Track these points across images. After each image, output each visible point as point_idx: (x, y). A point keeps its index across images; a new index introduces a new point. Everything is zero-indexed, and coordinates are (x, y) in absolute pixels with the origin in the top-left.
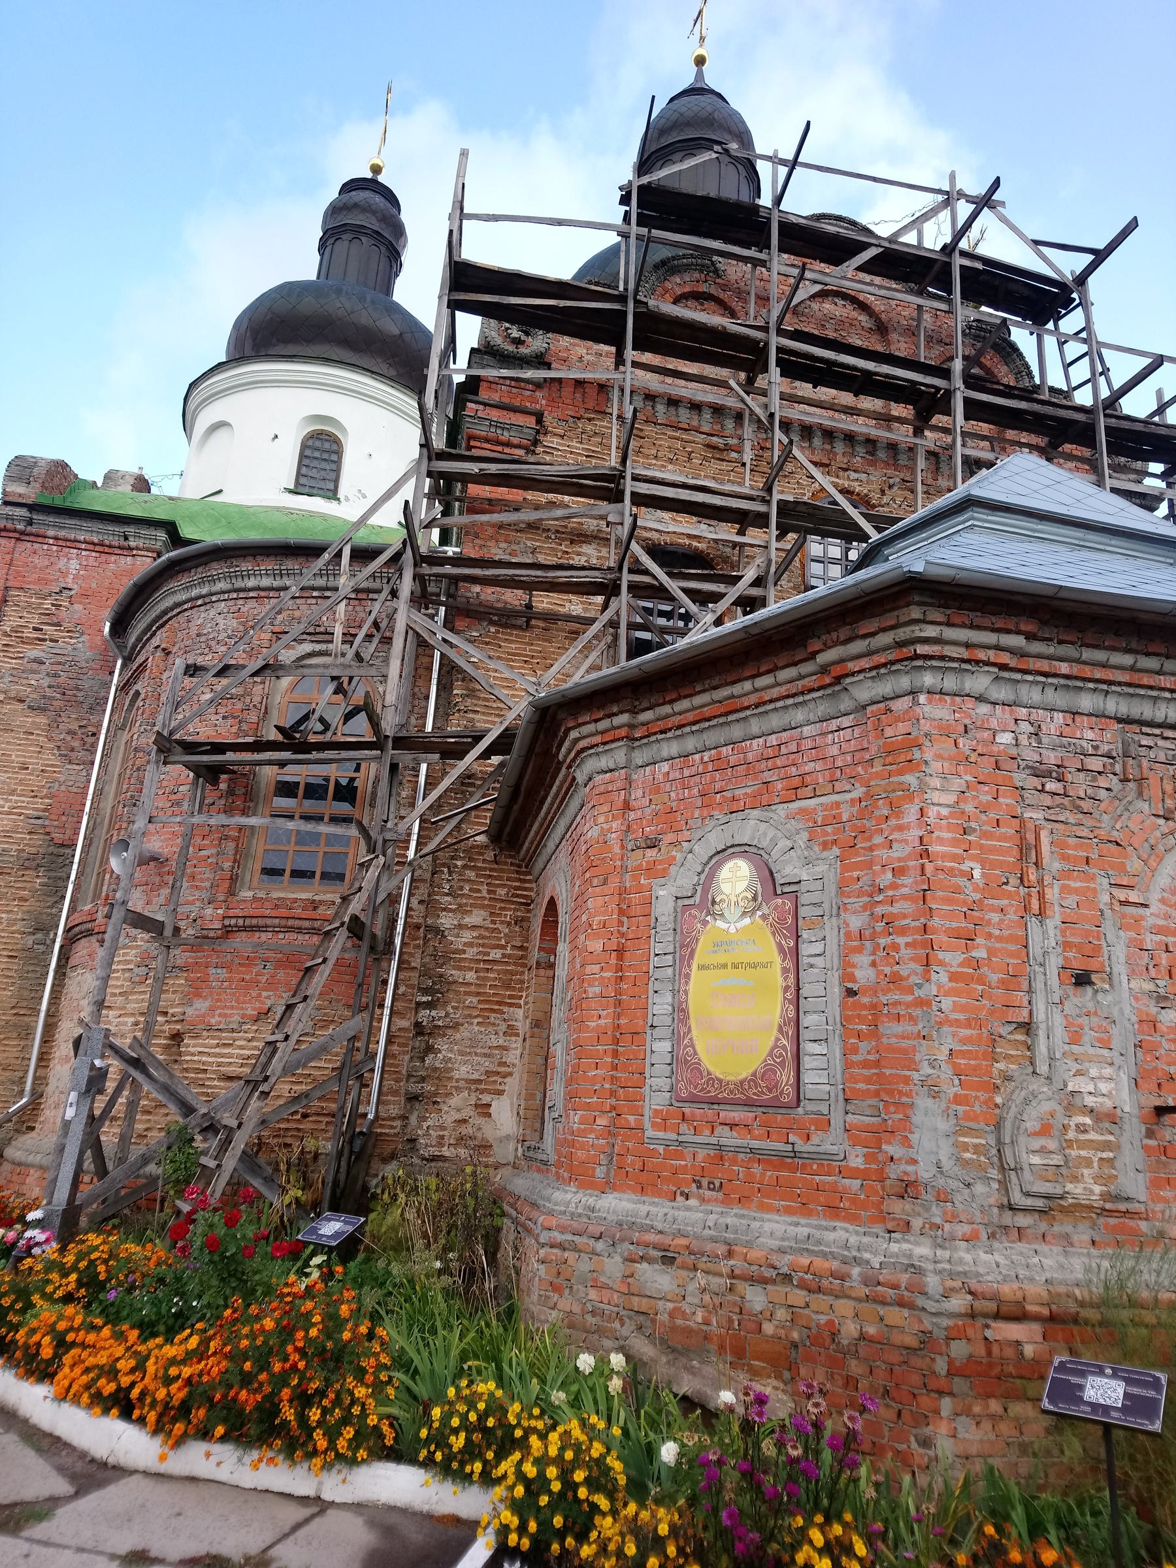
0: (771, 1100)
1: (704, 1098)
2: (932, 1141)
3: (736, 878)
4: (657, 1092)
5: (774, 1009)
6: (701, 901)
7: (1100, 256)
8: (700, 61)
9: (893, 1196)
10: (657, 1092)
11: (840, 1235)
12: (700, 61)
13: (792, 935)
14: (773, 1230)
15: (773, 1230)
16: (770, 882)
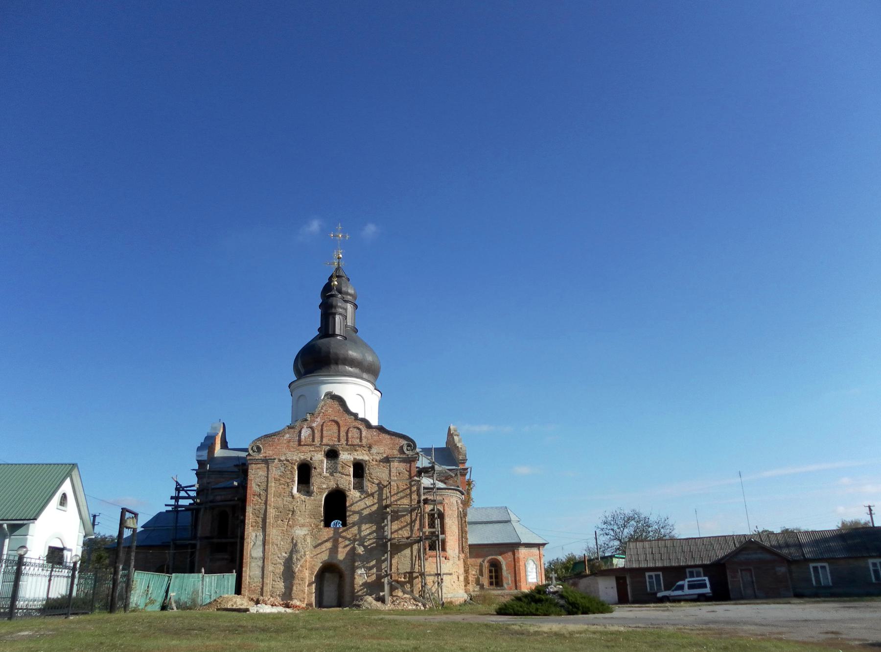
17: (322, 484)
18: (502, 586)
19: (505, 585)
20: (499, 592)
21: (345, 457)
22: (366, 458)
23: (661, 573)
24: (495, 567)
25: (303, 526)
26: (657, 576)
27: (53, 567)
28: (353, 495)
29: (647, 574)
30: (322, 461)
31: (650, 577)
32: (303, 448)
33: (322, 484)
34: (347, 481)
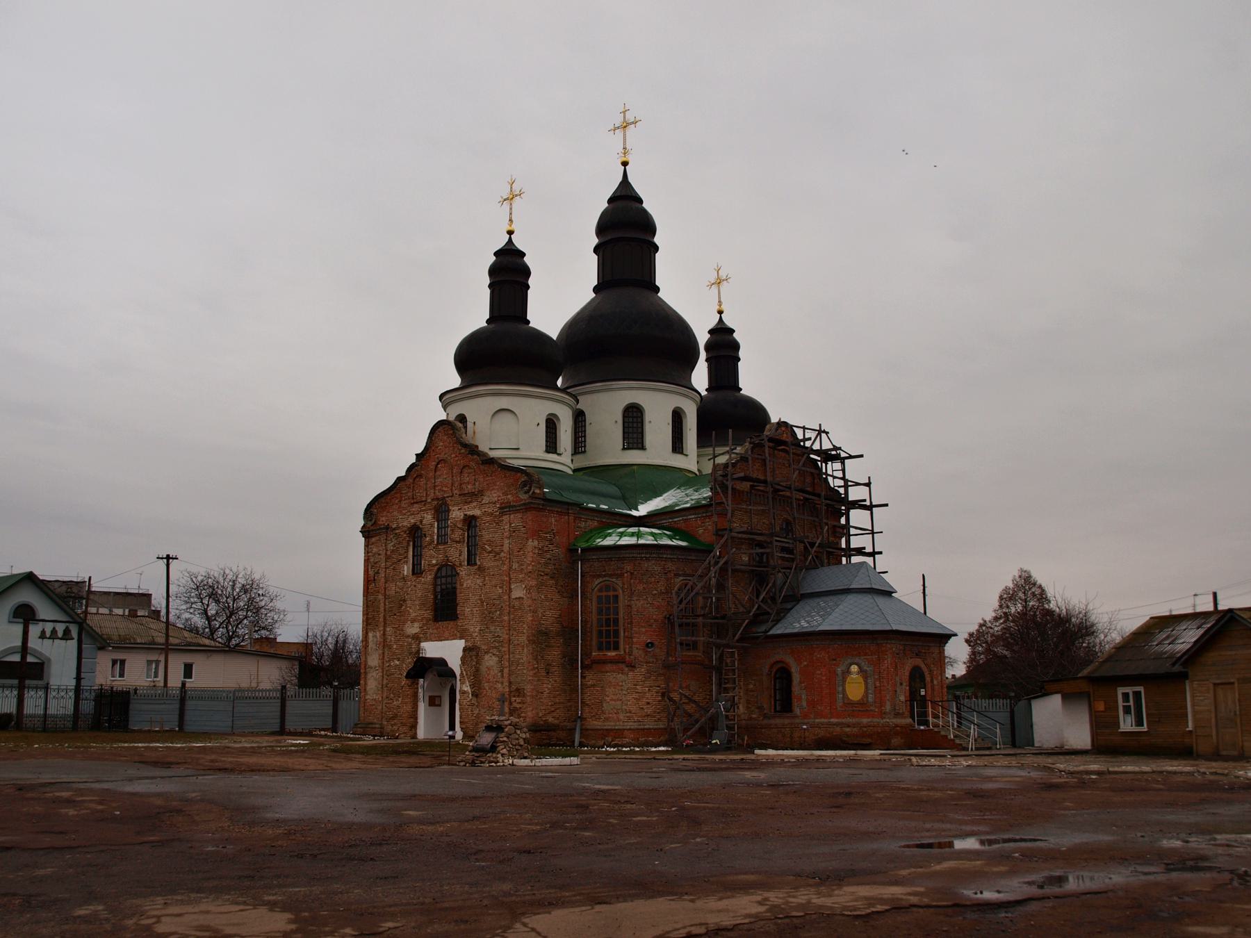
0: (862, 703)
1: (849, 704)
2: (888, 707)
3: (854, 668)
4: (839, 703)
5: (862, 690)
6: (848, 672)
7: (851, 457)
8: (625, 164)
9: (882, 714)
10: (839, 703)
11: (875, 720)
12: (625, 164)
13: (865, 678)
14: (865, 721)
15: (865, 721)
16: (861, 671)
17: (432, 558)
18: (791, 711)
19: (797, 711)
20: (787, 721)
21: (456, 514)
22: (477, 512)
23: (1141, 689)
24: (783, 675)
25: (413, 621)
26: (1137, 694)
27: (21, 689)
28: (463, 571)
29: (1121, 691)
30: (432, 525)
31: (1126, 696)
32: (416, 507)
33: (432, 558)
34: (457, 553)
